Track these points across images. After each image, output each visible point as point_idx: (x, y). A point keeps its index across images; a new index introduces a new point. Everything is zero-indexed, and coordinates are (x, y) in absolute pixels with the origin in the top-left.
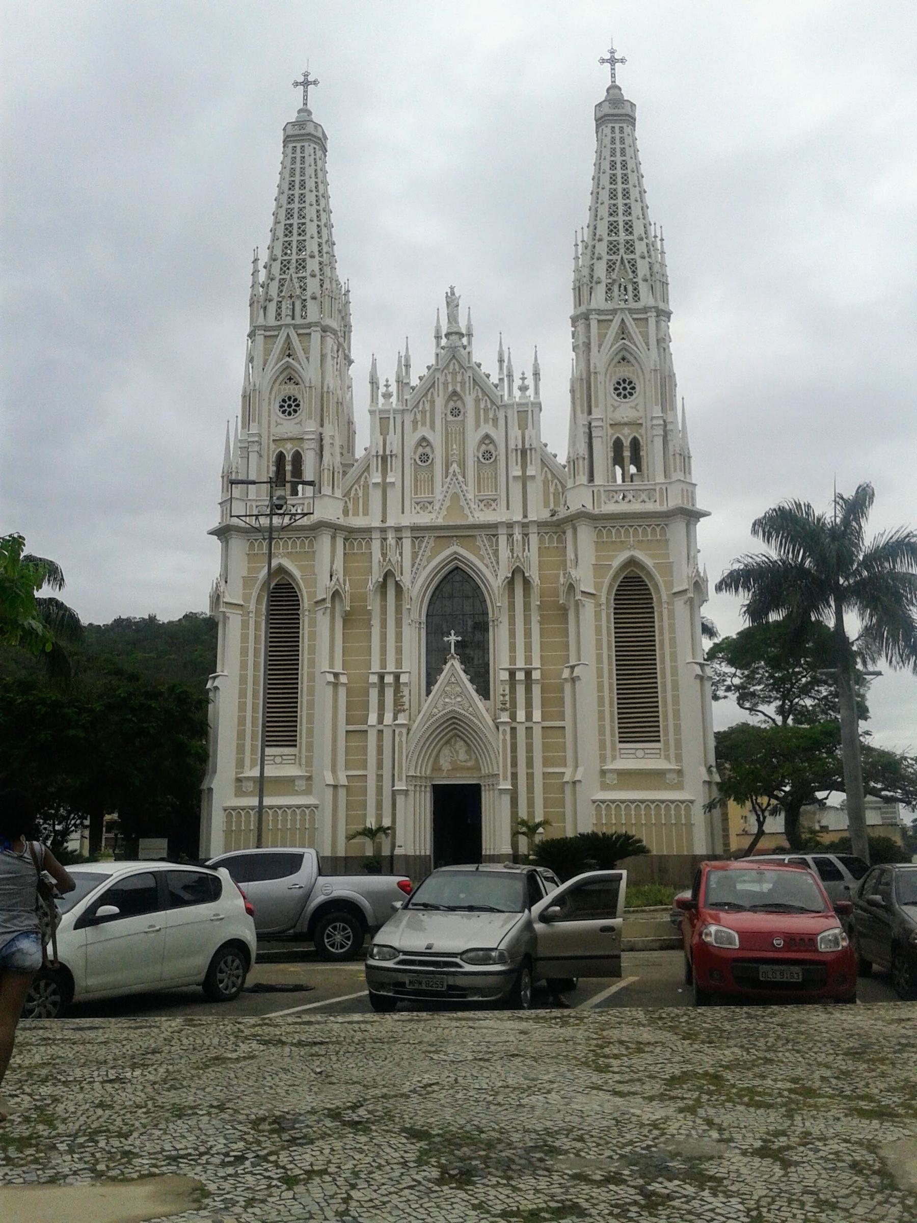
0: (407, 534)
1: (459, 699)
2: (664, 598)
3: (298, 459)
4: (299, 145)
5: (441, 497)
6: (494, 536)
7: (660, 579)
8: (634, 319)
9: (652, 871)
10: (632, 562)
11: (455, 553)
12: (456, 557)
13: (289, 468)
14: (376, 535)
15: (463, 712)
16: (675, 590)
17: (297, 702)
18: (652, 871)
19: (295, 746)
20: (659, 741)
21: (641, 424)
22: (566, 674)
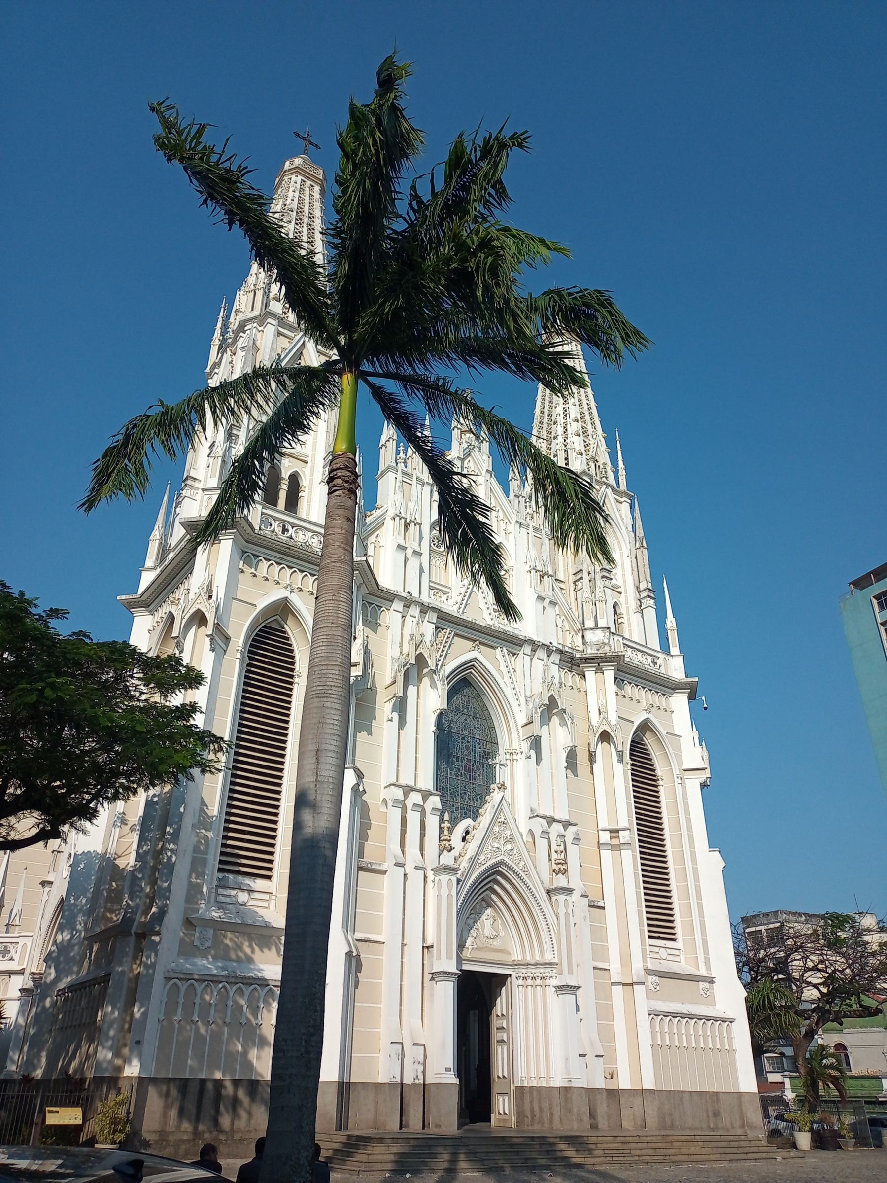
0: (434, 617)
1: (509, 847)
2: (676, 771)
3: (294, 479)
4: (308, 183)
5: (463, 590)
6: (514, 654)
7: (672, 752)
8: (616, 499)
9: (708, 1116)
10: (645, 727)
11: (475, 660)
12: (469, 665)
13: (284, 487)
14: (398, 605)
15: (513, 865)
16: (685, 767)
17: (277, 807)
18: (708, 1116)
19: (269, 878)
20: (674, 940)
21: (621, 593)
22: (605, 837)
